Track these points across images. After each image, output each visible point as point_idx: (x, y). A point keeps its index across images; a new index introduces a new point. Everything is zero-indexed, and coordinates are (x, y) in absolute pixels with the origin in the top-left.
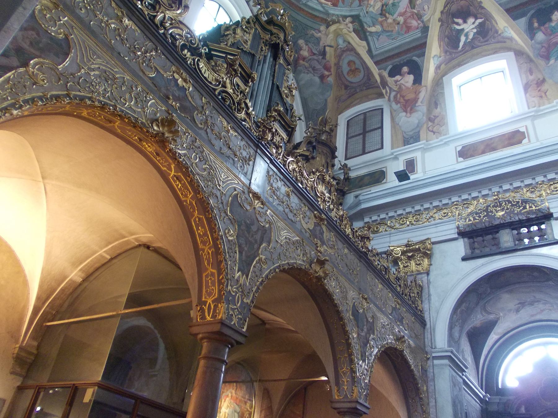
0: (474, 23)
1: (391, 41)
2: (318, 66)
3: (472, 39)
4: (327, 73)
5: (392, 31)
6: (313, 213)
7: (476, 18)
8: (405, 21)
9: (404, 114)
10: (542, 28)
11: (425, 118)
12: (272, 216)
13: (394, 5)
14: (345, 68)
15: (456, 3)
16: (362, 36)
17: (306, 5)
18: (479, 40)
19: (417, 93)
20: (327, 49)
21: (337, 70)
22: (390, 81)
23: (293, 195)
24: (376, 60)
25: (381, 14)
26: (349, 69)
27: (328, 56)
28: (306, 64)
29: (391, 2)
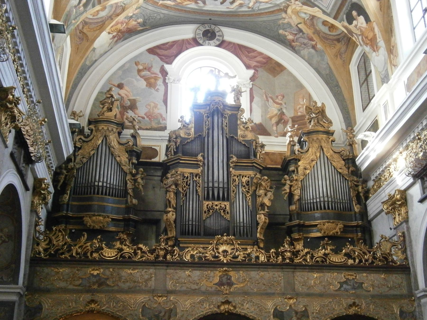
2: (306, 41)
4: (314, 43)
6: (217, 271)
9: (374, 54)
11: (386, 53)
12: (175, 299)
14: (325, 29)
16: (311, 4)
19: (373, 30)
20: (299, 26)
21: (319, 36)
22: (351, 27)
23: (195, 272)
26: (327, 28)
27: (304, 30)
28: (298, 44)
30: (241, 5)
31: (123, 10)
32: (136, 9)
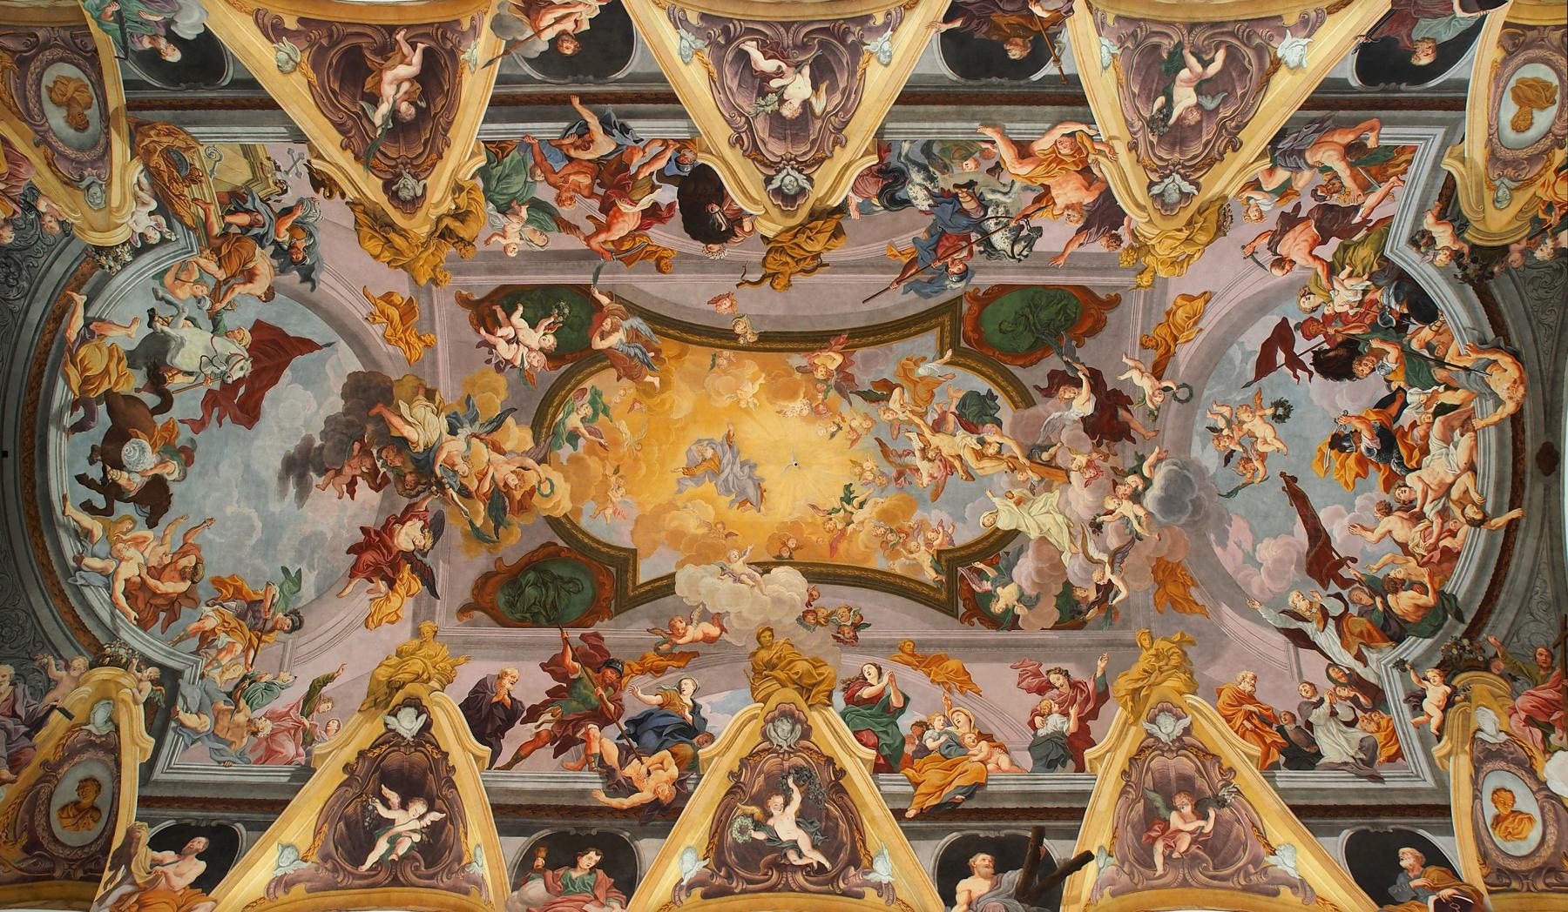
0: (421, 817)
1: (213, 765)
3: (403, 858)
5: (231, 744)
7: (431, 809)
8: (273, 734)
10: (549, 873)
13: (269, 687)
14: (67, 790)
15: (402, 749)
16: (157, 723)
17: (78, 591)
18: (417, 868)
22: (144, 854)
24: (148, 792)
25: (229, 695)
29: (268, 678)
30: (83, 535)
31: (68, 183)
32: (62, 223)
